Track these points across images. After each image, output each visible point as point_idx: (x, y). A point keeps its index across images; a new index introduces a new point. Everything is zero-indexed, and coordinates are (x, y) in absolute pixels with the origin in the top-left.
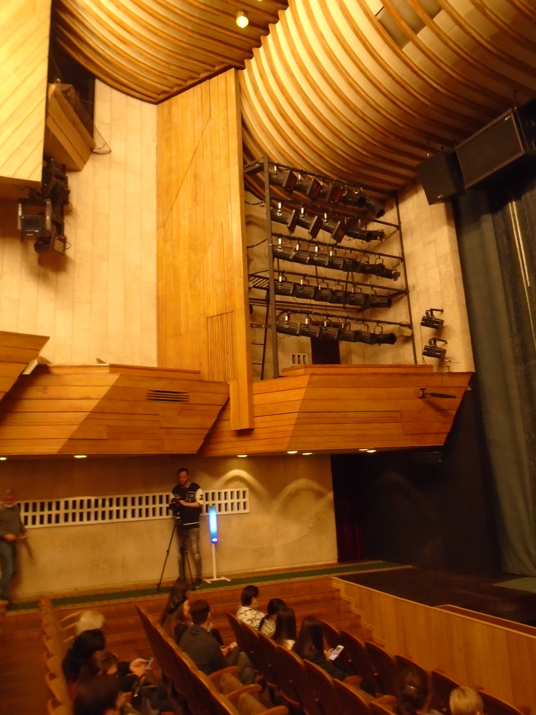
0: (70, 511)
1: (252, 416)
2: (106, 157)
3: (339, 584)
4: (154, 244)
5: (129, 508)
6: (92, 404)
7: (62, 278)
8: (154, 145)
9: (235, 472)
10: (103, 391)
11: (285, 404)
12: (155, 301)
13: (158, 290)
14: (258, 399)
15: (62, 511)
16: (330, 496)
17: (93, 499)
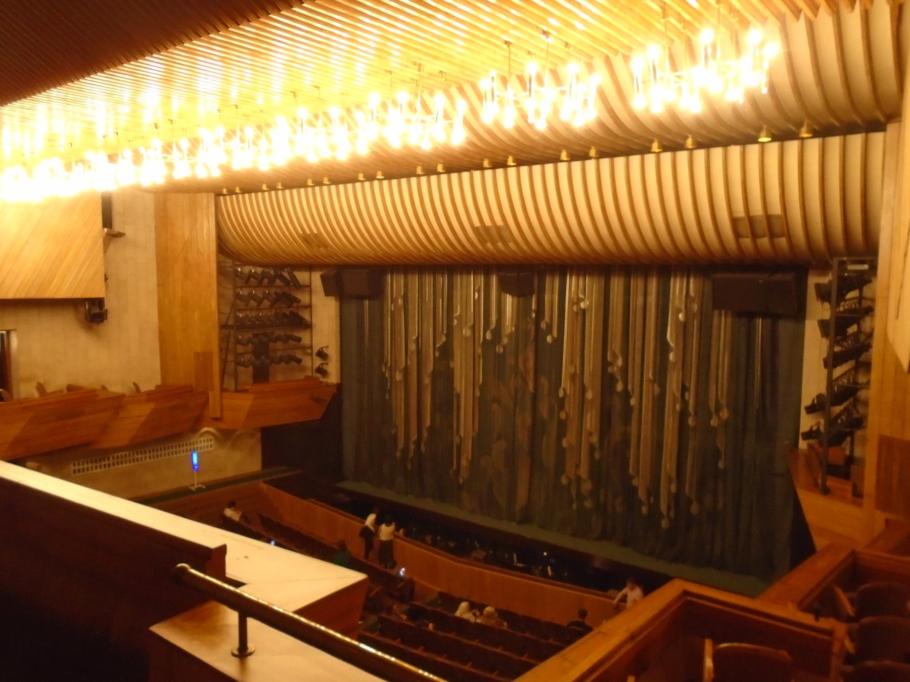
0: (116, 461)
1: (222, 410)
2: (122, 239)
3: (264, 486)
4: (156, 297)
5: (148, 455)
6: (143, 419)
7: (101, 327)
8: (153, 225)
9: (205, 429)
10: (148, 411)
11: (241, 405)
12: (157, 335)
13: (160, 328)
14: (225, 402)
15: (111, 461)
16: (259, 435)
17: (127, 453)
